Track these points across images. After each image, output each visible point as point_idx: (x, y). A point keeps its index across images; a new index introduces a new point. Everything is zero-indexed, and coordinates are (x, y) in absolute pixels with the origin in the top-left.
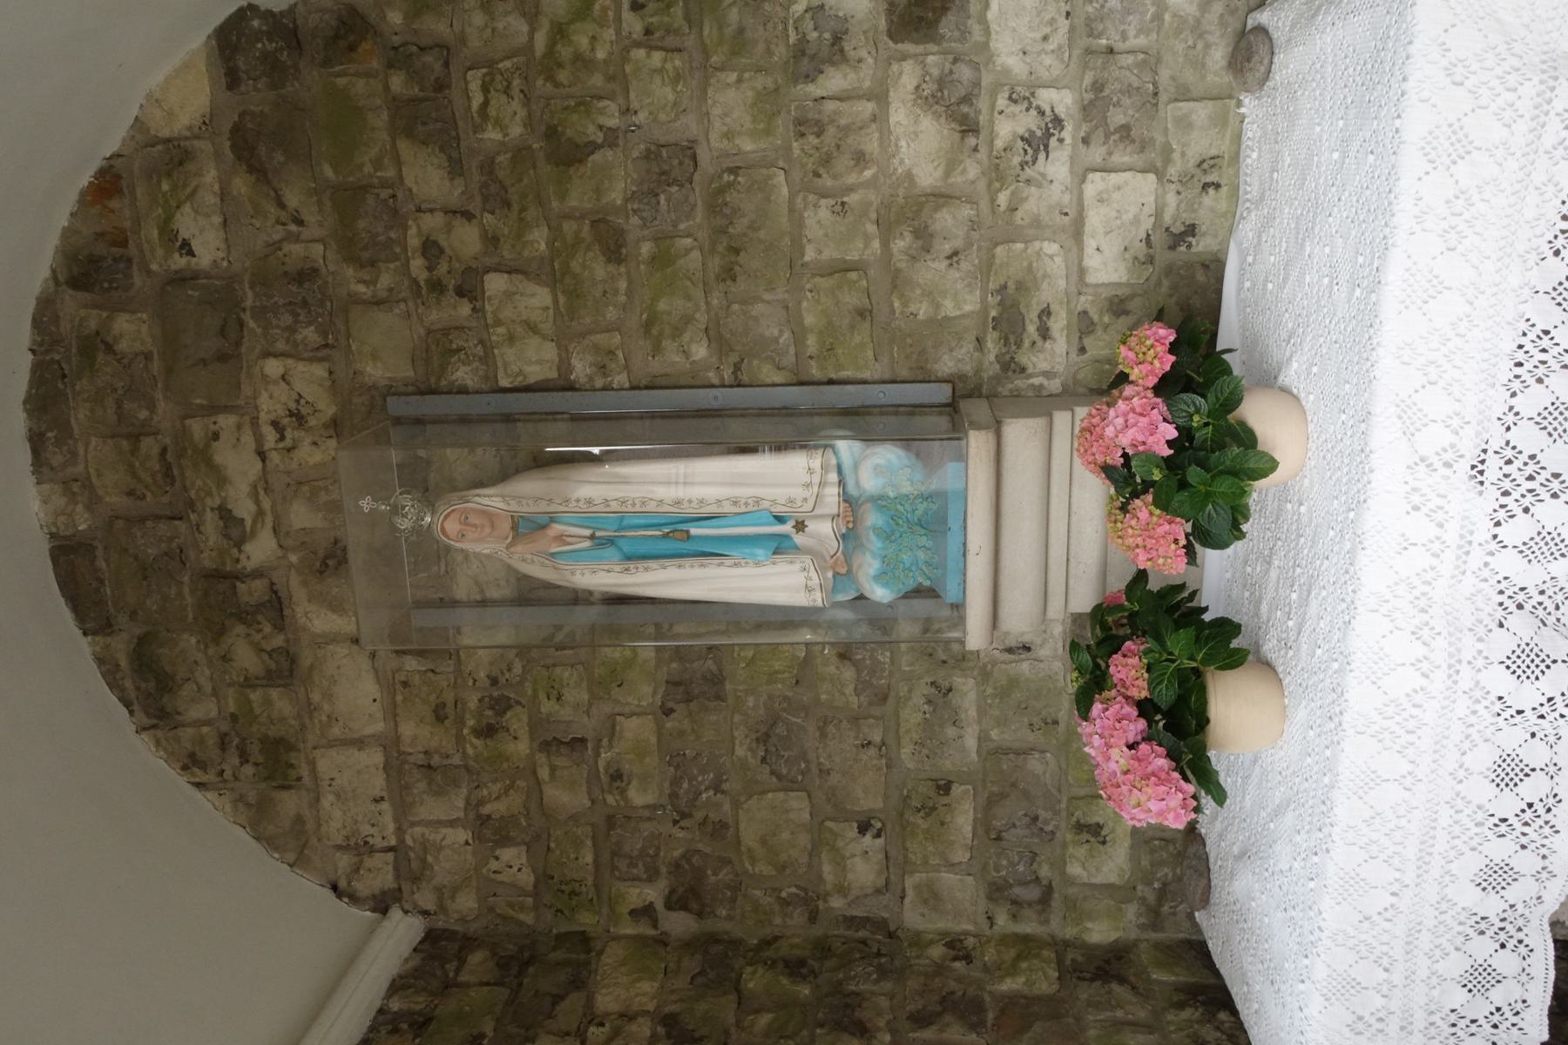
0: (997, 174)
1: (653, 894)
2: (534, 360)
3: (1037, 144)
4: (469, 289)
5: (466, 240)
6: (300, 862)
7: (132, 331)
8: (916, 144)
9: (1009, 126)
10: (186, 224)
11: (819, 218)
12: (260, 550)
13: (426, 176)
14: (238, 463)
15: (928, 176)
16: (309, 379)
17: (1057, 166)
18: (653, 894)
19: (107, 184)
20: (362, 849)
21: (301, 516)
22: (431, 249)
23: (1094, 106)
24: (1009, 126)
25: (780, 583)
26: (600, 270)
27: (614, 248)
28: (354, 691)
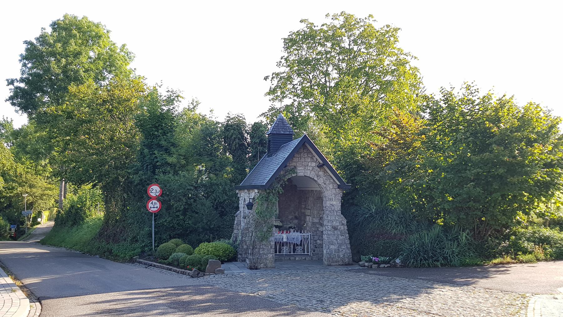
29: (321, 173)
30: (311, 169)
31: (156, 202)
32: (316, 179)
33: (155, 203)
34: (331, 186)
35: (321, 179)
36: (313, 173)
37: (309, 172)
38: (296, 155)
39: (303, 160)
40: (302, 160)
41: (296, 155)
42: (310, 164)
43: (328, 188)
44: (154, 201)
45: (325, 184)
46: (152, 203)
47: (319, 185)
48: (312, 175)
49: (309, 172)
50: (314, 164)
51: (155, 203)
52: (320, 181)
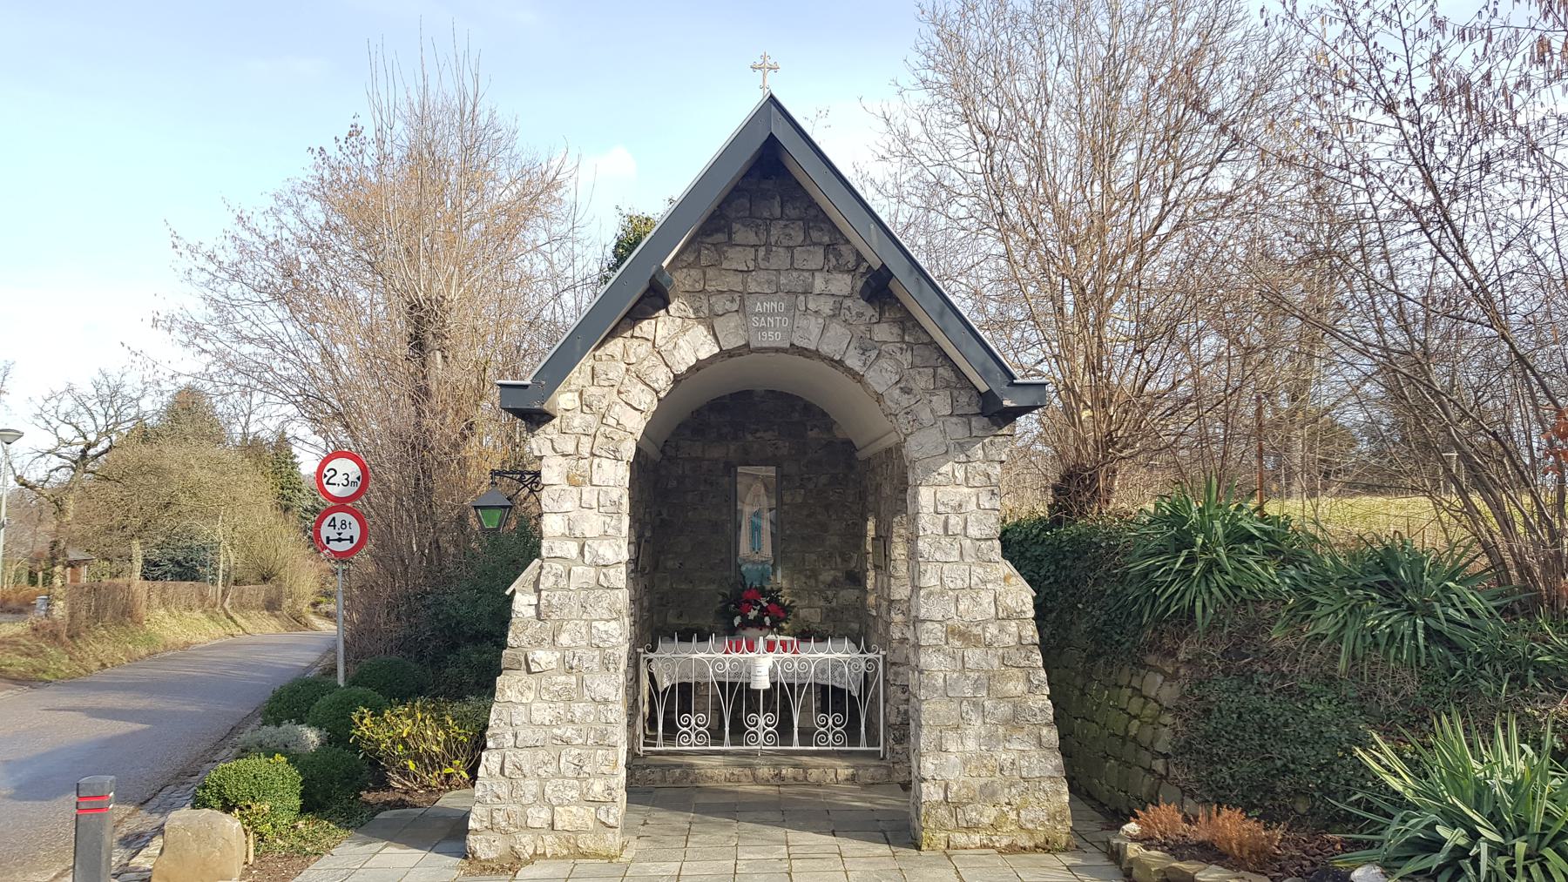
0: (820, 591)
1: (664, 515)
2: (787, 498)
3: (826, 599)
4: (802, 486)
5: (811, 486)
6: (673, 434)
7: (796, 416)
8: (827, 576)
9: (830, 593)
10: (816, 430)
11: (814, 557)
12: (749, 437)
13: (824, 480)
14: (768, 435)
15: (821, 578)
16: (785, 451)
17: (822, 603)
18: (664, 515)
19: (825, 414)
20: (677, 448)
21: (756, 446)
22: (810, 479)
23: (833, 610)
24: (830, 593)
25: (744, 548)
26: (805, 512)
27: (808, 516)
28: (716, 453)
29: (885, 333)
30: (826, 307)
31: (349, 518)
32: (853, 362)
33: (343, 523)
34: (942, 403)
35: (885, 363)
36: (836, 329)
37: (814, 325)
38: (742, 234)
39: (780, 258)
40: (775, 263)
41: (742, 234)
42: (819, 283)
43: (926, 416)
44: (340, 516)
45: (907, 391)
46: (333, 525)
47: (879, 398)
48: (836, 342)
49: (814, 325)
50: (842, 284)
51: (343, 523)
52: (881, 377)
